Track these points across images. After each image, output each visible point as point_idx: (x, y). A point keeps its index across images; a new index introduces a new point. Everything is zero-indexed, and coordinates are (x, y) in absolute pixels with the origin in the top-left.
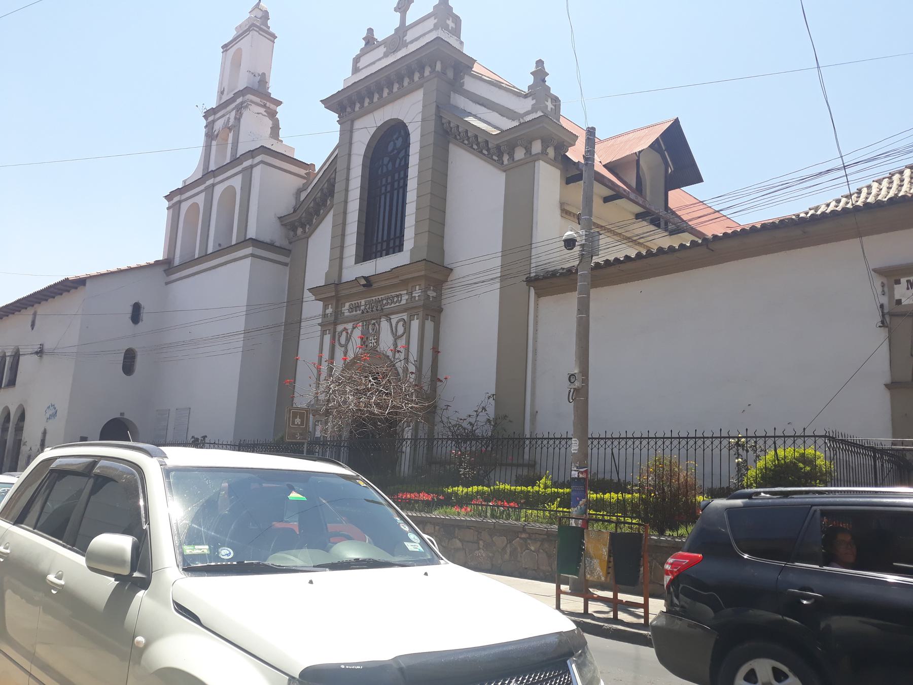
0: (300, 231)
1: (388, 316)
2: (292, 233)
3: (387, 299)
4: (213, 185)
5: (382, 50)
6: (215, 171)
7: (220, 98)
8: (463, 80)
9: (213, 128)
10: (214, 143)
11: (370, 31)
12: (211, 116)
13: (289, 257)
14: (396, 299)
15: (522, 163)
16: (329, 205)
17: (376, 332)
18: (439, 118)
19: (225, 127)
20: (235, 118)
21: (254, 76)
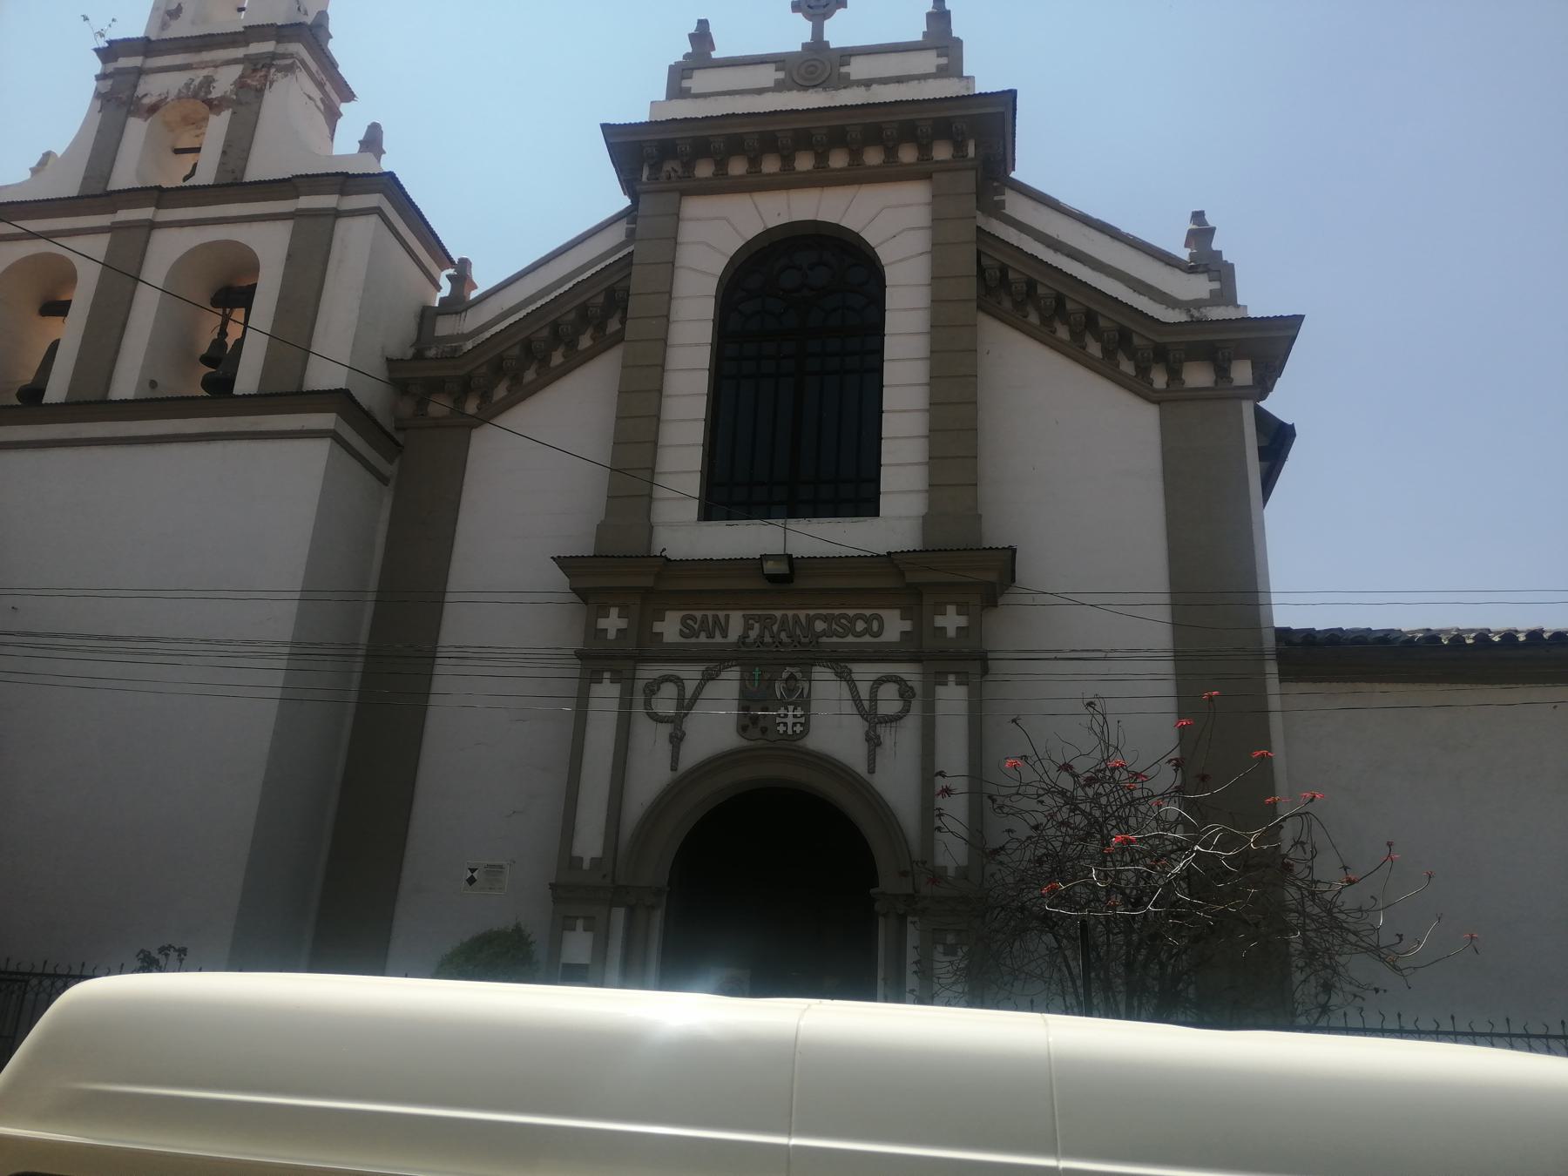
0: (439, 407)
1: (840, 661)
2: (407, 408)
4: (152, 225)
5: (768, 75)
6: (168, 190)
7: (164, 26)
8: (1003, 198)
9: (135, 87)
10: (137, 129)
11: (703, 24)
12: (136, 54)
13: (391, 461)
14: (860, 626)
15: (1198, 395)
16: (558, 366)
17: (799, 696)
18: (979, 253)
19: (195, 96)
20: (241, 84)
21: (299, 9)
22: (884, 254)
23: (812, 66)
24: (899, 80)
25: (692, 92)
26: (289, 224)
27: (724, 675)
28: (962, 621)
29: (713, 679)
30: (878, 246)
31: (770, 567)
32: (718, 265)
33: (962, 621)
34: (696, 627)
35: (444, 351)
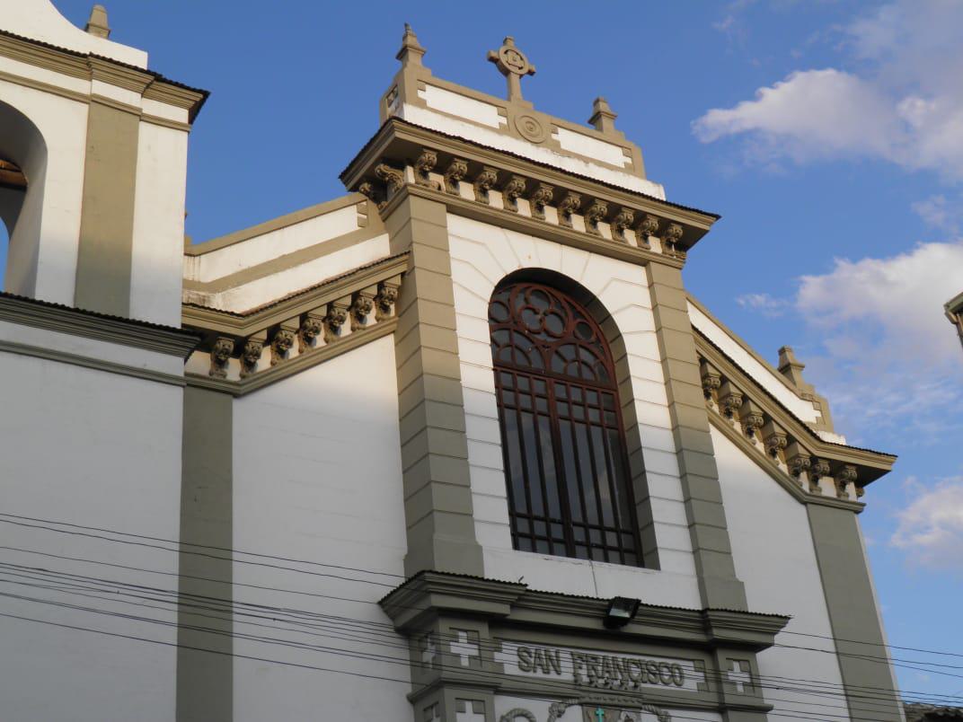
1: (662, 705)
3: (638, 664)
5: (489, 115)
22: (623, 322)
23: (533, 124)
24: (600, 164)
25: (429, 105)
26: (85, 108)
27: (568, 710)
28: (746, 678)
29: (559, 716)
30: (616, 312)
31: (615, 612)
32: (487, 292)
33: (746, 678)
34: (532, 660)
35: (189, 298)
